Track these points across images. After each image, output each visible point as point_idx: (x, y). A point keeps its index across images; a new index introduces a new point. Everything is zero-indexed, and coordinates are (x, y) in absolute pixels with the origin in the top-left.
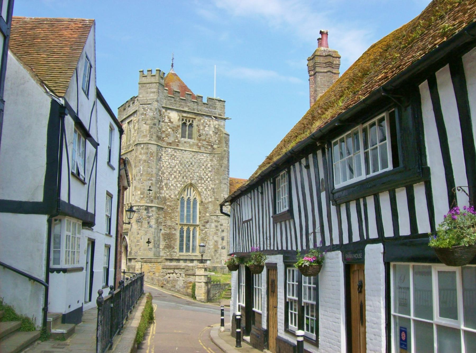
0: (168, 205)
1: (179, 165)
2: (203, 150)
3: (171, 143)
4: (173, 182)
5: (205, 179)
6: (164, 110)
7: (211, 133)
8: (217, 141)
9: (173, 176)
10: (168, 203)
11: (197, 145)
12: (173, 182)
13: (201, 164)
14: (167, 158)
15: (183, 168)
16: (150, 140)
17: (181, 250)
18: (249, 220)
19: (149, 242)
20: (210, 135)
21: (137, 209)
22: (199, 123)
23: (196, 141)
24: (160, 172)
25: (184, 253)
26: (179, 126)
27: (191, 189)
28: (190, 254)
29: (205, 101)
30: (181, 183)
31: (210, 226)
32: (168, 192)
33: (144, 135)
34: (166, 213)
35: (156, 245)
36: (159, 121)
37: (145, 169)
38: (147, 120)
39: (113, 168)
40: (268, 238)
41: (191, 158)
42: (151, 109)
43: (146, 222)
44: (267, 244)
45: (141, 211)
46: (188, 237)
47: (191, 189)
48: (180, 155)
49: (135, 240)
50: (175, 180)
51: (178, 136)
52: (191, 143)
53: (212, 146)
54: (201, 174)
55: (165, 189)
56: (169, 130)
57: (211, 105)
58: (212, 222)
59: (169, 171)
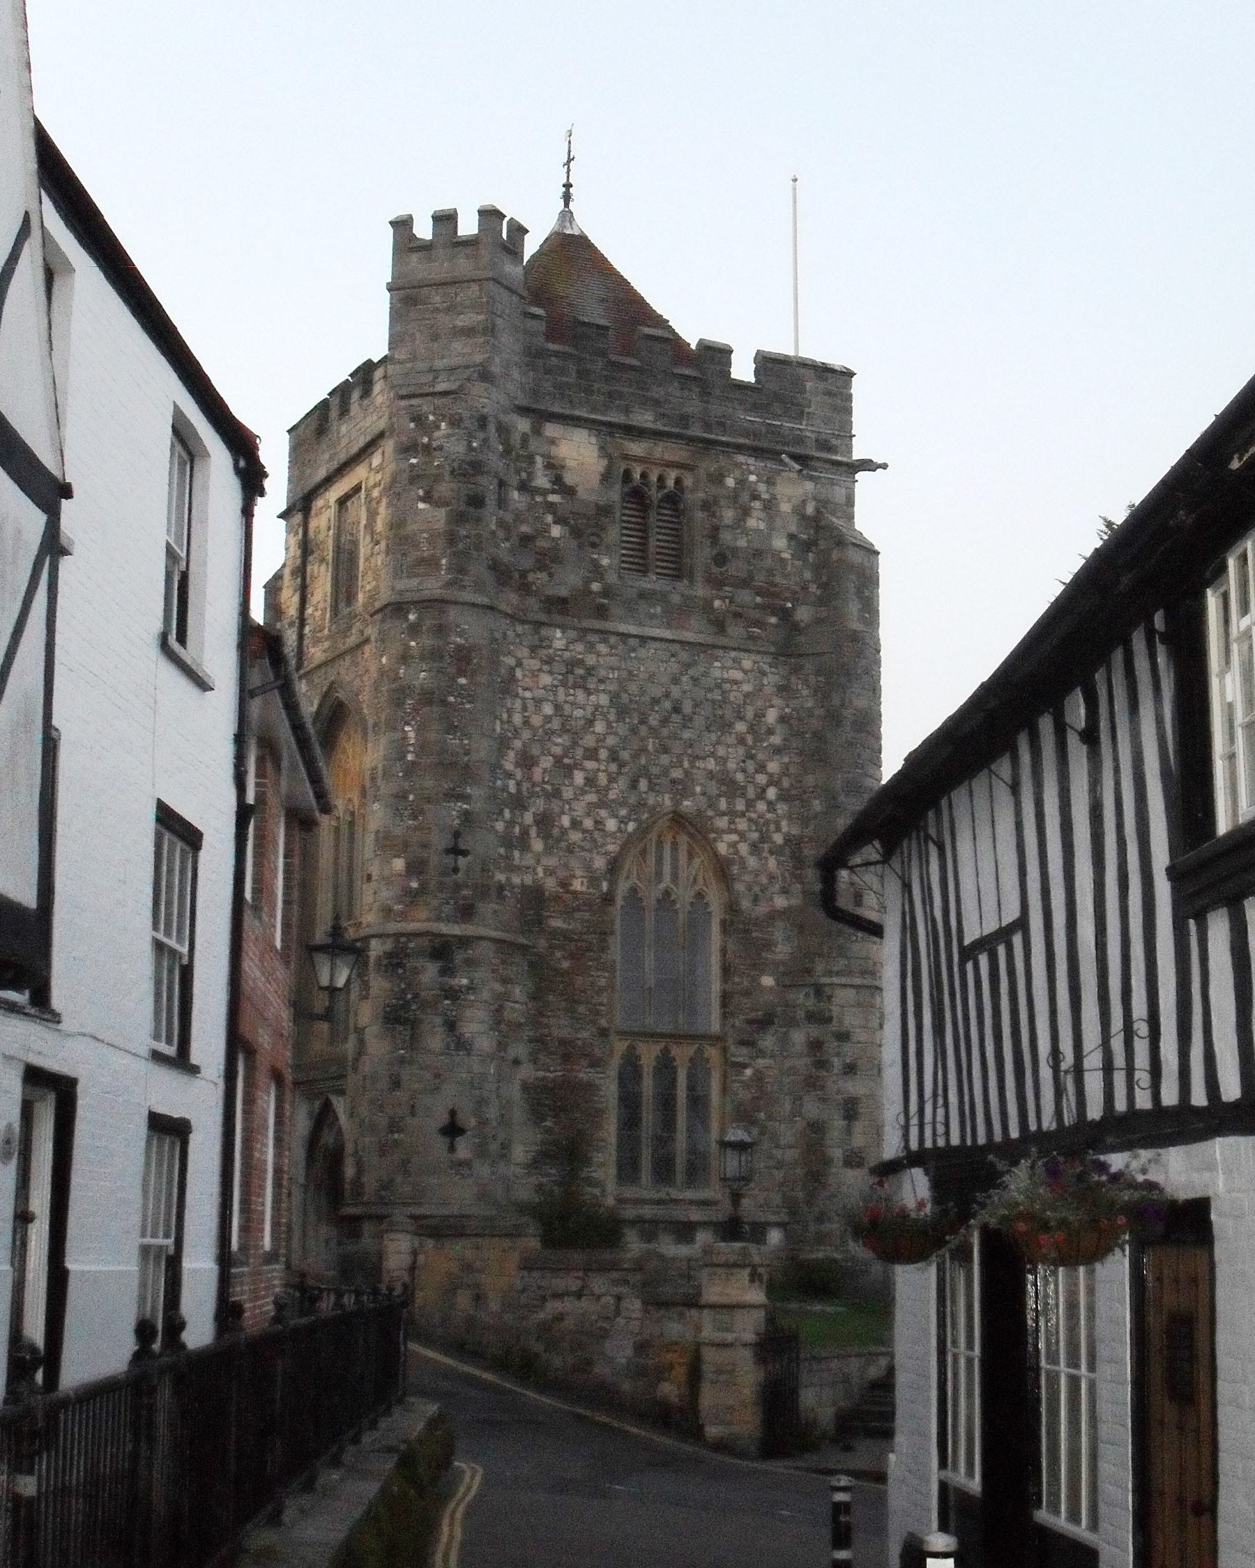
0: (555, 933)
1: (612, 717)
2: (736, 631)
3: (564, 601)
4: (579, 808)
5: (751, 792)
7: (780, 543)
8: (813, 588)
9: (579, 778)
10: (557, 923)
11: (707, 606)
12: (579, 808)
13: (728, 713)
14: (546, 679)
15: (634, 731)
16: (449, 584)
17: (628, 1169)
18: (1003, 934)
19: (452, 1130)
20: (776, 554)
21: (389, 955)
22: (714, 490)
23: (701, 591)
24: (511, 754)
25: (646, 1188)
26: (604, 511)
27: (675, 847)
28: (675, 1194)
29: (743, 370)
30: (623, 812)
31: (784, 1040)
32: (551, 861)
33: (421, 561)
35: (494, 1147)
36: (502, 484)
37: (432, 736)
38: (438, 478)
39: (202, 684)
40: (1142, 1028)
41: (676, 681)
42: (455, 422)
43: (438, 1020)
44: (1130, 1070)
45: (410, 963)
46: (666, 1103)
47: (675, 847)
48: (613, 661)
49: (382, 1121)
50: (592, 797)
51: (605, 561)
52: (676, 599)
53: (785, 615)
54: (731, 765)
55: (538, 845)
56: (556, 531)
57: (777, 397)
58: (792, 1023)
59: (558, 750)
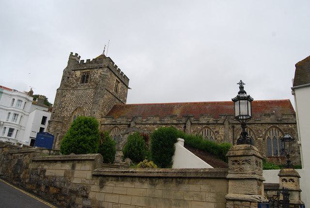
2: (91, 87)
6: (73, 72)
26: (79, 78)
34: (63, 124)
